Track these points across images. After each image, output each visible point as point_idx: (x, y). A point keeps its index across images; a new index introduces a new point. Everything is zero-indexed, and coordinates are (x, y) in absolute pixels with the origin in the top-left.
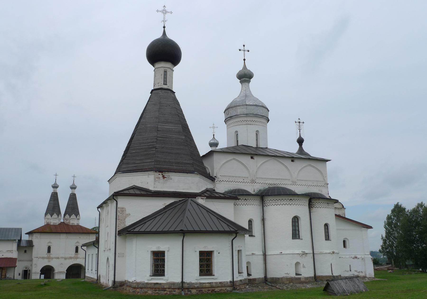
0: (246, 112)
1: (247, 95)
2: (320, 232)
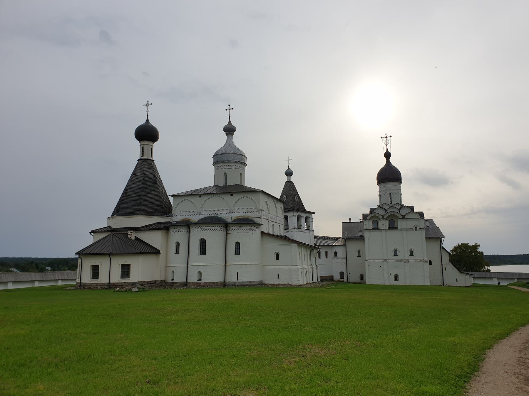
0: (228, 159)
1: (229, 144)
2: (232, 248)
